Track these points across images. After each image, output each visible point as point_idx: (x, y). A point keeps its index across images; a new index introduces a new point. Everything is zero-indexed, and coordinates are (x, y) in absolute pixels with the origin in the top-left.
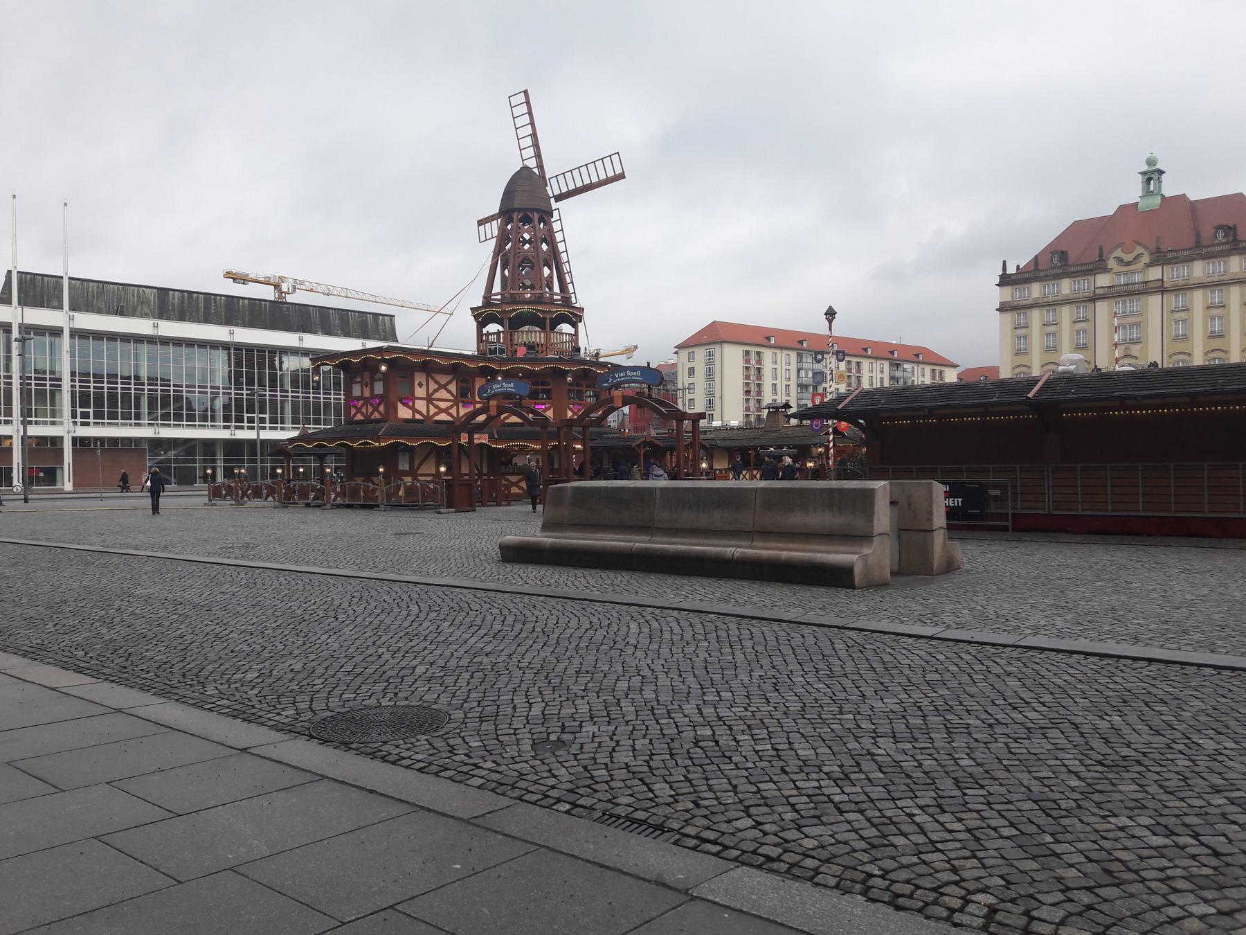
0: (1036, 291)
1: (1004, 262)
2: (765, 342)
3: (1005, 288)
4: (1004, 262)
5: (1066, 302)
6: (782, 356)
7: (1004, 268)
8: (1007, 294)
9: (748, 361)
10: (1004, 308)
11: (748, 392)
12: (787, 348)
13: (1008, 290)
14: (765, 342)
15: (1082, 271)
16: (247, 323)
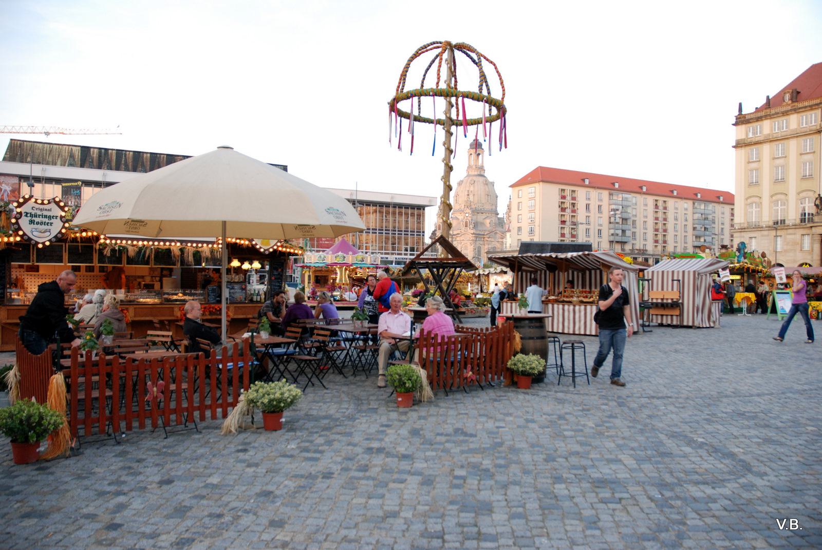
0: (766, 127)
1: (740, 105)
2: (670, 194)
3: (739, 127)
4: (740, 105)
5: (796, 135)
6: (594, 193)
7: (740, 109)
8: (741, 132)
9: (563, 197)
10: (739, 145)
11: (563, 222)
12: (598, 188)
13: (743, 128)
14: (581, 183)
15: (811, 106)
16: (130, 167)
